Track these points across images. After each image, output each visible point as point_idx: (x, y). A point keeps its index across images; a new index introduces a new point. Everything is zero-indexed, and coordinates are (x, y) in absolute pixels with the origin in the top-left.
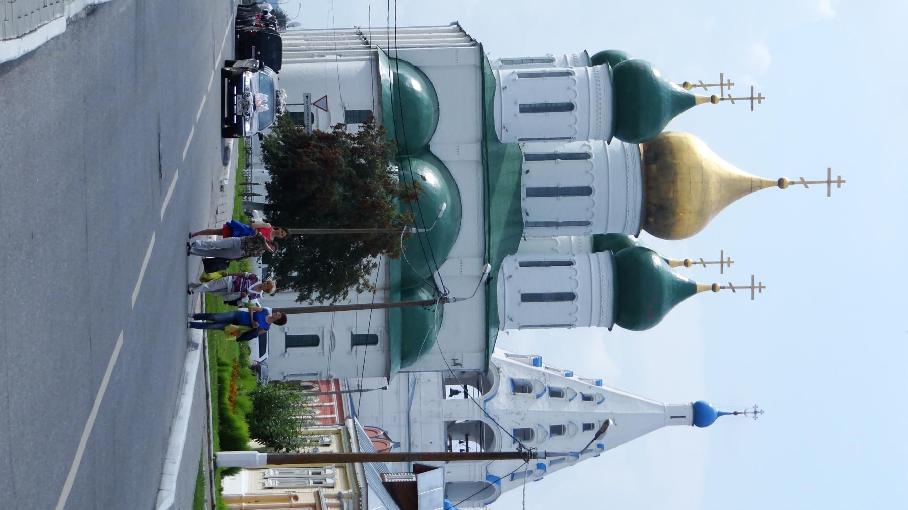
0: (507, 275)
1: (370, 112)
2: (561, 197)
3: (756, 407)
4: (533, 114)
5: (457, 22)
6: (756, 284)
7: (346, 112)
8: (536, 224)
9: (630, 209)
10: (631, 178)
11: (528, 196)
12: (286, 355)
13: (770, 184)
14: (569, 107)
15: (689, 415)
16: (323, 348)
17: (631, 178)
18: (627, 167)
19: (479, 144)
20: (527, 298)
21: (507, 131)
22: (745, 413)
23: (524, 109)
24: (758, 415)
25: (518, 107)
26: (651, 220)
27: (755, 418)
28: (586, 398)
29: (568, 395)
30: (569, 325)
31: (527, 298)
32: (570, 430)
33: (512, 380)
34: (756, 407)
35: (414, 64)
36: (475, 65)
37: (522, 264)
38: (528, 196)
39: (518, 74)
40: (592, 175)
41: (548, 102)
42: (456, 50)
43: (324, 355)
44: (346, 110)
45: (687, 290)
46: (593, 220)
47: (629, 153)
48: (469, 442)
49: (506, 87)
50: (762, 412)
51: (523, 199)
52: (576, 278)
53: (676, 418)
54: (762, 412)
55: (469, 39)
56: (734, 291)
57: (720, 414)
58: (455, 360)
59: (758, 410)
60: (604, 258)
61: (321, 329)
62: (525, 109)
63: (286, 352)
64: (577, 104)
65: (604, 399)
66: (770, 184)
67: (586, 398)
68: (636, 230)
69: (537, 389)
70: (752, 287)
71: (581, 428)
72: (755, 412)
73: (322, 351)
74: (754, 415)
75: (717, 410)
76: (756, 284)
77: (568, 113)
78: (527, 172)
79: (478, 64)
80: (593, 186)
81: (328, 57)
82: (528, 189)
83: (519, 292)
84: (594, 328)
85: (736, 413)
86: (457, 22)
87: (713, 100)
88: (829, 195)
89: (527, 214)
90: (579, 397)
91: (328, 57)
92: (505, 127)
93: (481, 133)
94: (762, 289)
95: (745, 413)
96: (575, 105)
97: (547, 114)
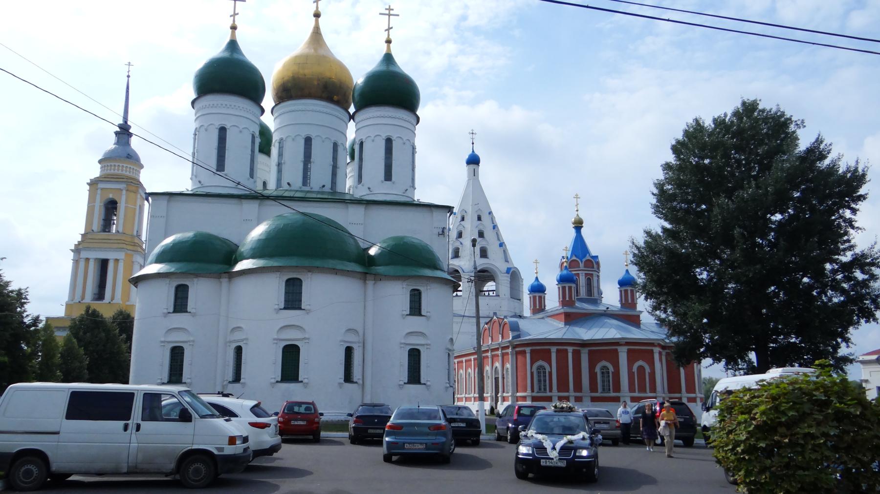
0: (368, 192)
3: (470, 133)
6: (387, 12)
7: (175, 311)
9: (325, 110)
10: (300, 107)
12: (428, 383)
13: (317, 22)
14: (223, 131)
15: (472, 166)
16: (423, 345)
17: (300, 107)
19: (243, 200)
20: (388, 176)
22: (473, 139)
24: (474, 132)
27: (476, 134)
28: (463, 219)
29: (461, 228)
31: (388, 176)
32: (481, 228)
34: (470, 133)
36: (169, 201)
40: (295, 136)
42: (151, 216)
43: (429, 345)
46: (333, 140)
47: (282, 111)
48: (484, 290)
49: (200, 182)
50: (472, 130)
51: (311, 189)
52: (373, 137)
53: (475, 173)
54: (472, 130)
56: (392, 28)
57: (473, 151)
58: (439, 234)
59: (471, 132)
61: (402, 346)
63: (425, 384)
64: (220, 123)
65: (463, 210)
66: (317, 22)
67: (463, 219)
70: (389, 15)
71: (479, 222)
72: (473, 133)
73: (426, 347)
74: (474, 135)
75: (471, 152)
76: (387, 12)
77: (228, 131)
78: (289, 184)
79: (167, 197)
80: (304, 134)
83: (383, 182)
89: (324, 186)
90: (462, 223)
93: (233, 199)
95: (473, 139)
96: (221, 126)
97: (227, 148)
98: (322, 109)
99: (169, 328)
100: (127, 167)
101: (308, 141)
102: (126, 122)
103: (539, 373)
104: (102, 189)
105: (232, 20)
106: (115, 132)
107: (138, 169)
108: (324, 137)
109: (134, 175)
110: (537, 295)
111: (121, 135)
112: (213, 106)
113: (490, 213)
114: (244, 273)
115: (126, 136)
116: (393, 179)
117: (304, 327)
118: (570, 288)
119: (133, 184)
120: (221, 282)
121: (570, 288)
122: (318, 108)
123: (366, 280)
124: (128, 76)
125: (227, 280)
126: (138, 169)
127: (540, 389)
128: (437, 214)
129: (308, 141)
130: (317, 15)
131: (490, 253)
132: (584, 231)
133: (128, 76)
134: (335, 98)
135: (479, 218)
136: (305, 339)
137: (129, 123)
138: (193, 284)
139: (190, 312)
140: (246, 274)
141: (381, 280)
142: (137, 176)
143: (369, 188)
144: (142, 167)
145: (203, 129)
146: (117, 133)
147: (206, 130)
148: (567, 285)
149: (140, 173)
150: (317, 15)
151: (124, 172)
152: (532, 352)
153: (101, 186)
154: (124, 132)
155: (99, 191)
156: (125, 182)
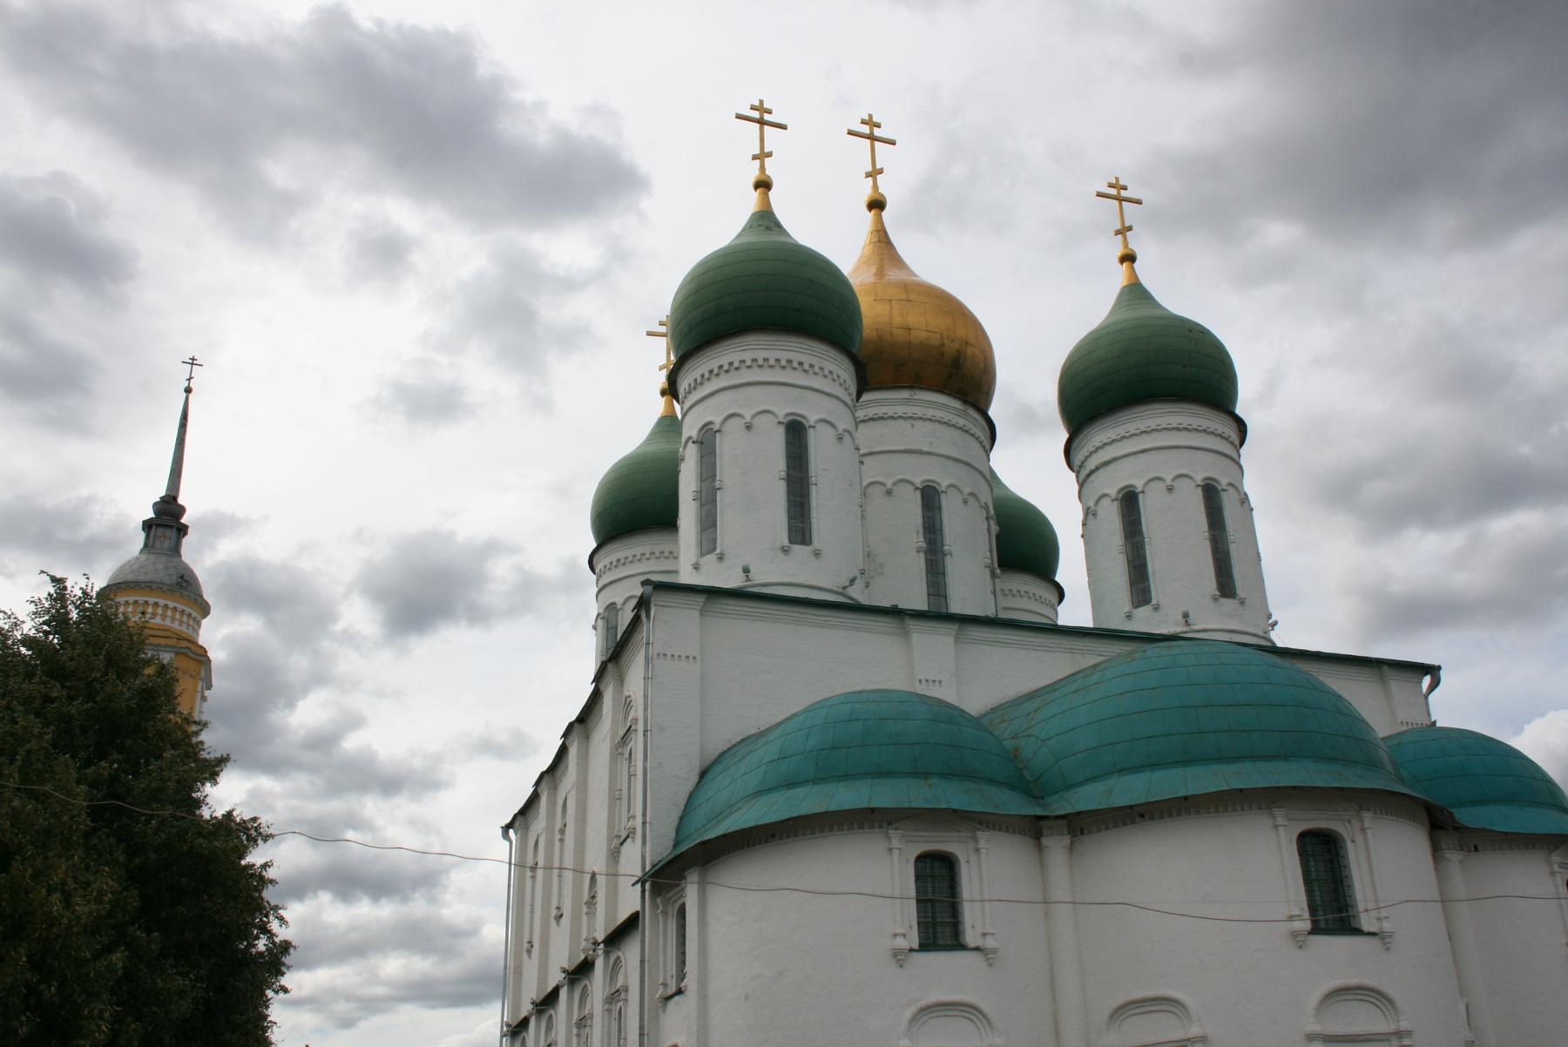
1: (921, 859)
2: (946, 548)
4: (814, 514)
5: (502, 827)
18: (876, 416)
21: (853, 581)
23: (800, 527)
25: (796, 548)
35: (695, 779)
36: (703, 612)
39: (702, 555)
40: (895, 484)
41: (783, 474)
44: (916, 945)
52: (1168, 479)
55: (577, 726)
62: (800, 527)
64: (789, 411)
79: (700, 600)
86: (502, 827)
88: (893, 143)
92: (844, 588)
94: (1122, 182)
99: (923, 1003)
100: (175, 608)
102: (175, 498)
105: (758, 166)
106: (144, 522)
107: (199, 617)
109: (190, 631)
111: (160, 531)
112: (765, 364)
114: (1142, 816)
115: (172, 533)
116: (1241, 592)
117: (1391, 993)
119: (191, 655)
120: (1040, 848)
123: (1441, 849)
124: (188, 390)
125: (1067, 840)
126: (199, 617)
128: (1398, 686)
129: (930, 497)
133: (188, 390)
136: (1399, 1034)
137: (181, 501)
138: (977, 850)
139: (977, 949)
140: (1152, 818)
141: (1476, 849)
142: (195, 636)
143: (1186, 615)
144: (205, 610)
145: (735, 424)
147: (749, 427)
149: (199, 624)
151: (168, 622)
156: (174, 647)
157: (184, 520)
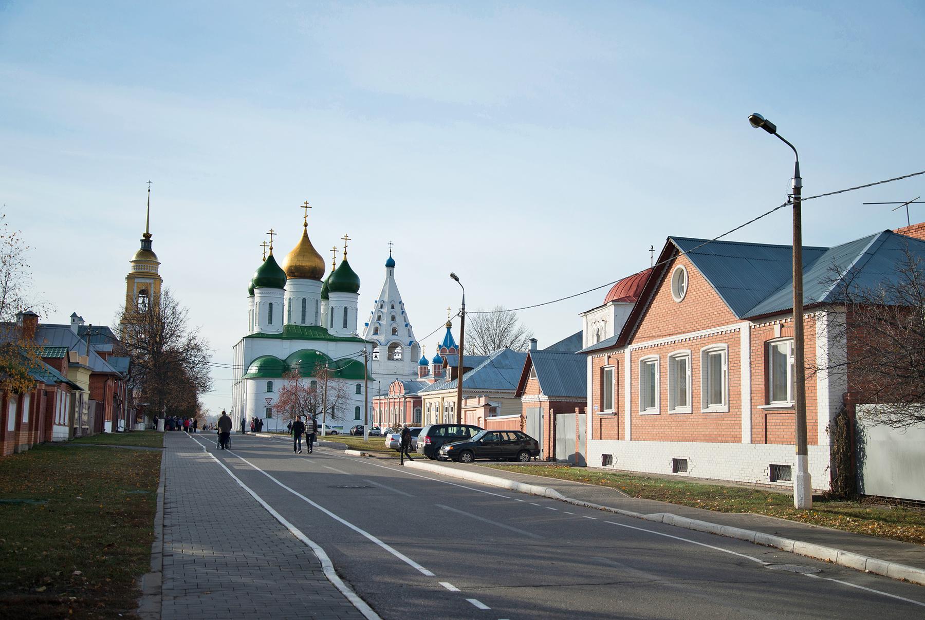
8: (316, 321)
11: (305, 323)
13: (306, 230)
14: (271, 305)
15: (391, 268)
19: (283, 340)
20: (345, 326)
26: (317, 276)
30: (357, 310)
31: (345, 326)
32: (393, 314)
33: (373, 334)
37: (332, 327)
38: (305, 323)
45: (345, 264)
50: (391, 241)
53: (391, 274)
54: (391, 241)
60: (330, 295)
68: (320, 282)
69: (377, 325)
70: (346, 239)
71: (393, 310)
81: (245, 398)
82: (302, 323)
84: (358, 301)
85: (391, 251)
87: (271, 249)
90: (381, 310)
91: (245, 398)
98: (312, 284)
101: (304, 300)
103: (417, 413)
104: (137, 283)
108: (312, 298)
110: (423, 366)
113: (400, 302)
118: (439, 366)
121: (439, 366)
122: (309, 284)
127: (417, 421)
130: (306, 225)
131: (399, 332)
132: (451, 330)
134: (317, 276)
135: (393, 307)
146: (142, 241)
148: (437, 365)
150: (306, 225)
152: (414, 402)
153: (137, 280)
154: (147, 240)
155: (136, 284)
157: (151, 239)
